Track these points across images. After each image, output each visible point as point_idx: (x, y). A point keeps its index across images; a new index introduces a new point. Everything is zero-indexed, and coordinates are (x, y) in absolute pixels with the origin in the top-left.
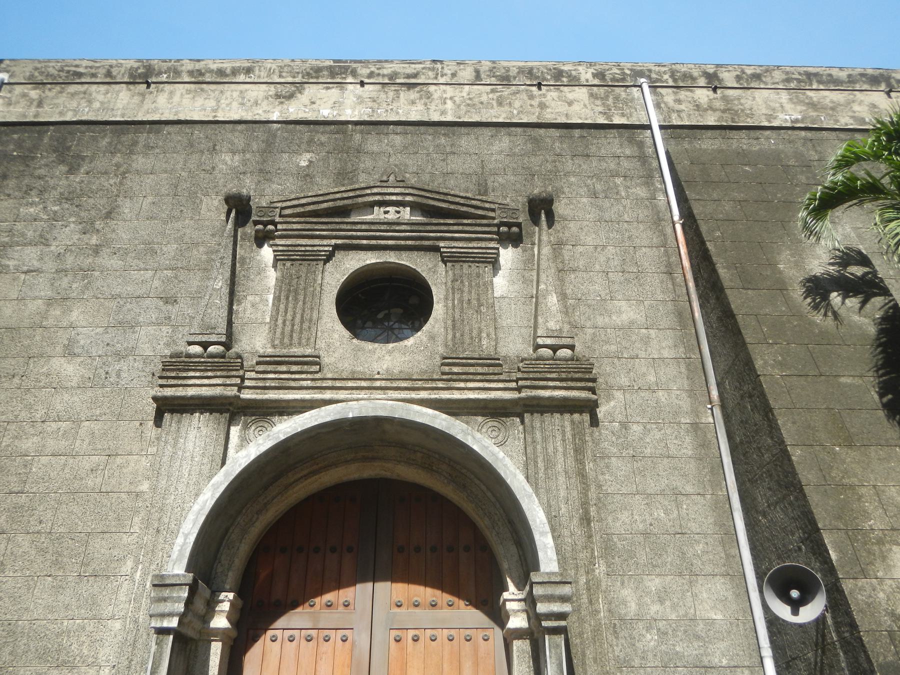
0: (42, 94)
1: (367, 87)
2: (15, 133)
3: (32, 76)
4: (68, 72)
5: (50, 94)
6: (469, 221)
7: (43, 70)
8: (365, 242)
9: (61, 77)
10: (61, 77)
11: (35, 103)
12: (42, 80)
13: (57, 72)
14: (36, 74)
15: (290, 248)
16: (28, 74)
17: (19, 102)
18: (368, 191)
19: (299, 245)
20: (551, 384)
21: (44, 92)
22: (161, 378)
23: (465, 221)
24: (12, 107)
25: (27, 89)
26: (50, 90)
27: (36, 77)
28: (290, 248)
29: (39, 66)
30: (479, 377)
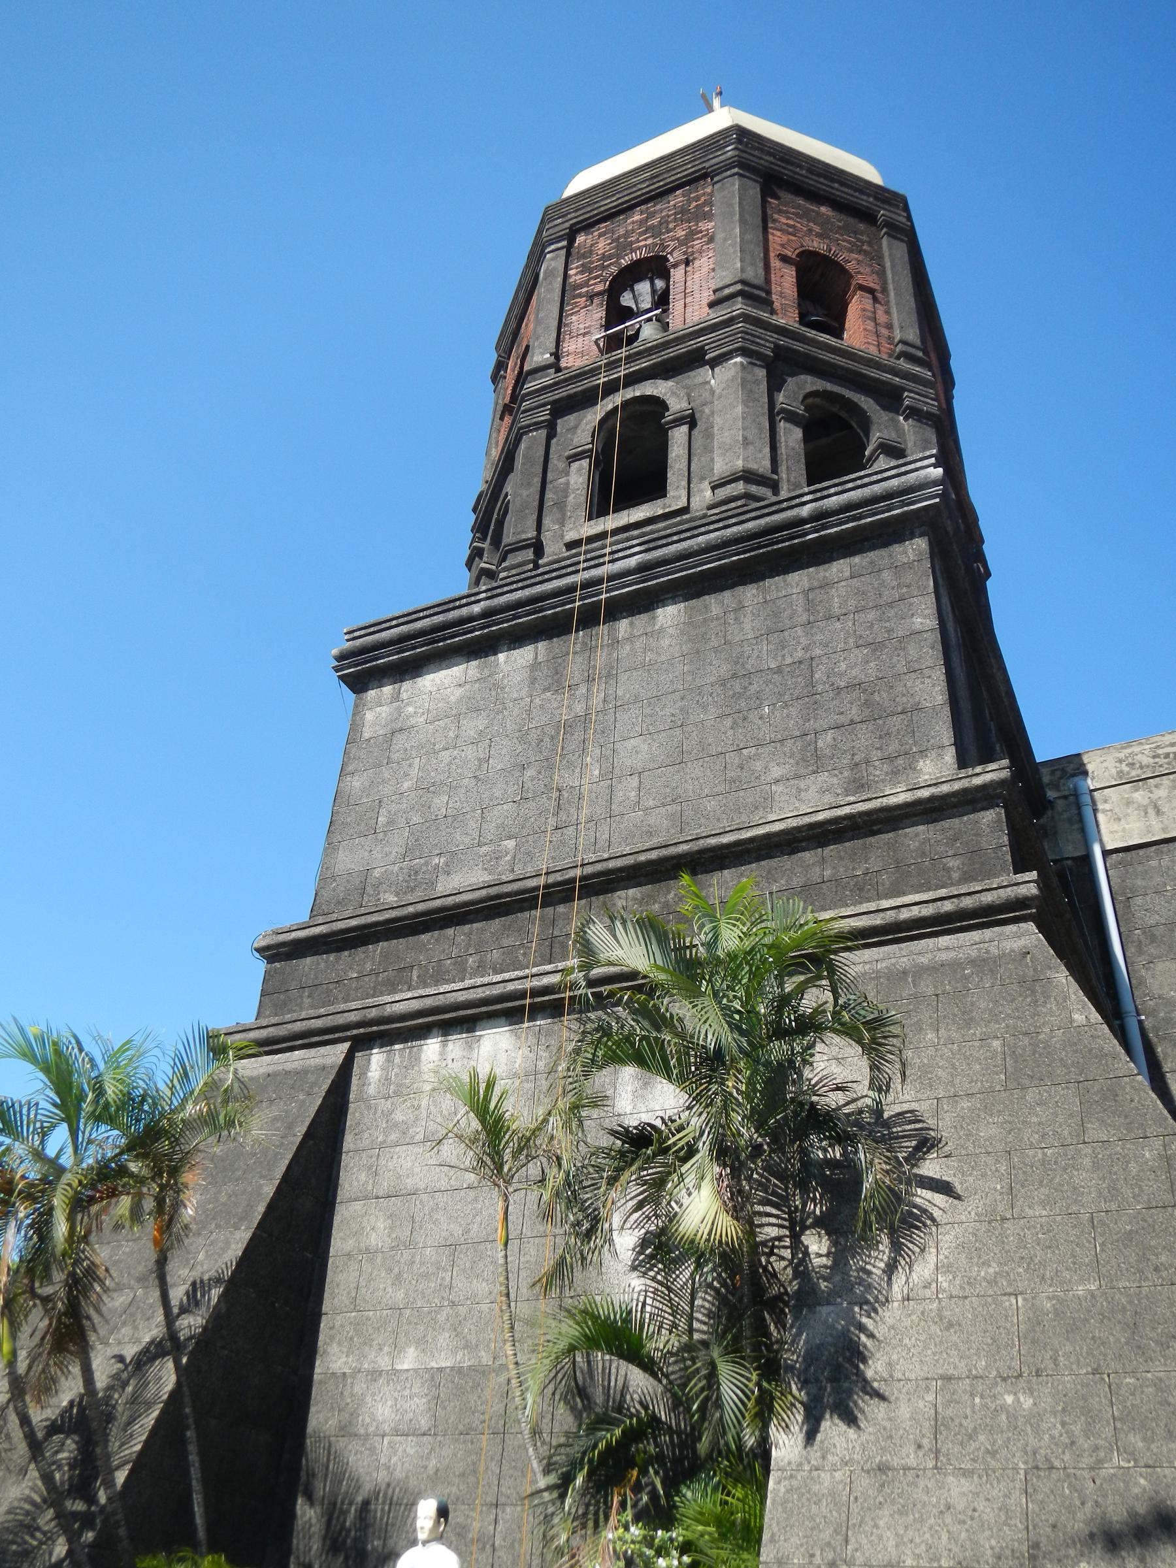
0: (1151, 795)
2: (1149, 858)
3: (1120, 773)
4: (1167, 755)
5: (1162, 793)
7: (1130, 760)
9: (1161, 766)
10: (1161, 766)
11: (1151, 811)
12: (1138, 776)
13: (1151, 761)
14: (1126, 769)
16: (1114, 771)
17: (1128, 815)
21: (1151, 792)
24: (1123, 821)
25: (1125, 791)
26: (1156, 786)
27: (1128, 773)
29: (1122, 755)
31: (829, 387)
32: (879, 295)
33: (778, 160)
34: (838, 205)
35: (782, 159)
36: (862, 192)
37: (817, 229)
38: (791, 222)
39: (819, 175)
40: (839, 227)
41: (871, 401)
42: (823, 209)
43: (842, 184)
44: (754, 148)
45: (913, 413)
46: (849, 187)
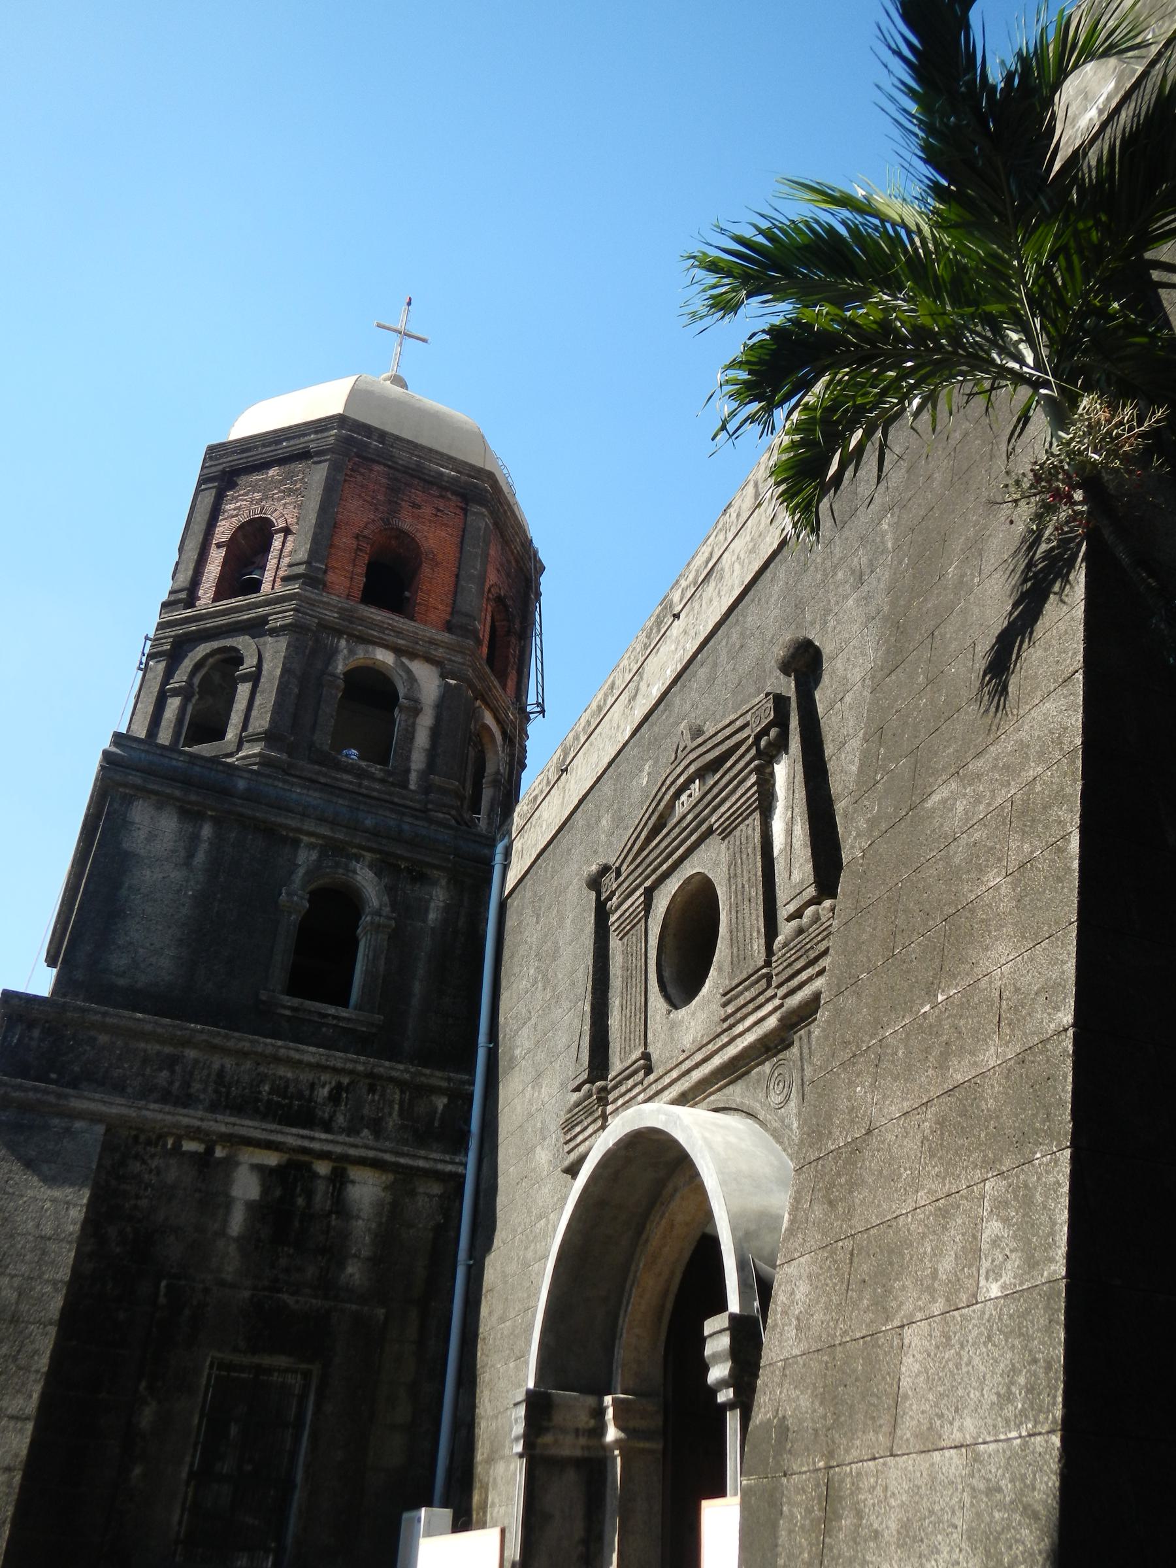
1: (682, 615)
6: (733, 759)
8: (665, 867)
15: (621, 920)
18: (664, 789)
19: (626, 911)
20: (804, 976)
22: (566, 1143)
23: (728, 764)
28: (621, 920)
30: (751, 1006)
31: (216, 644)
32: (294, 528)
33: (239, 453)
34: (280, 462)
35: (243, 451)
36: (305, 435)
37: (258, 495)
38: (238, 504)
39: (270, 444)
40: (280, 481)
41: (247, 637)
42: (271, 473)
43: (287, 439)
44: (221, 456)
45: (274, 632)
46: (293, 438)
